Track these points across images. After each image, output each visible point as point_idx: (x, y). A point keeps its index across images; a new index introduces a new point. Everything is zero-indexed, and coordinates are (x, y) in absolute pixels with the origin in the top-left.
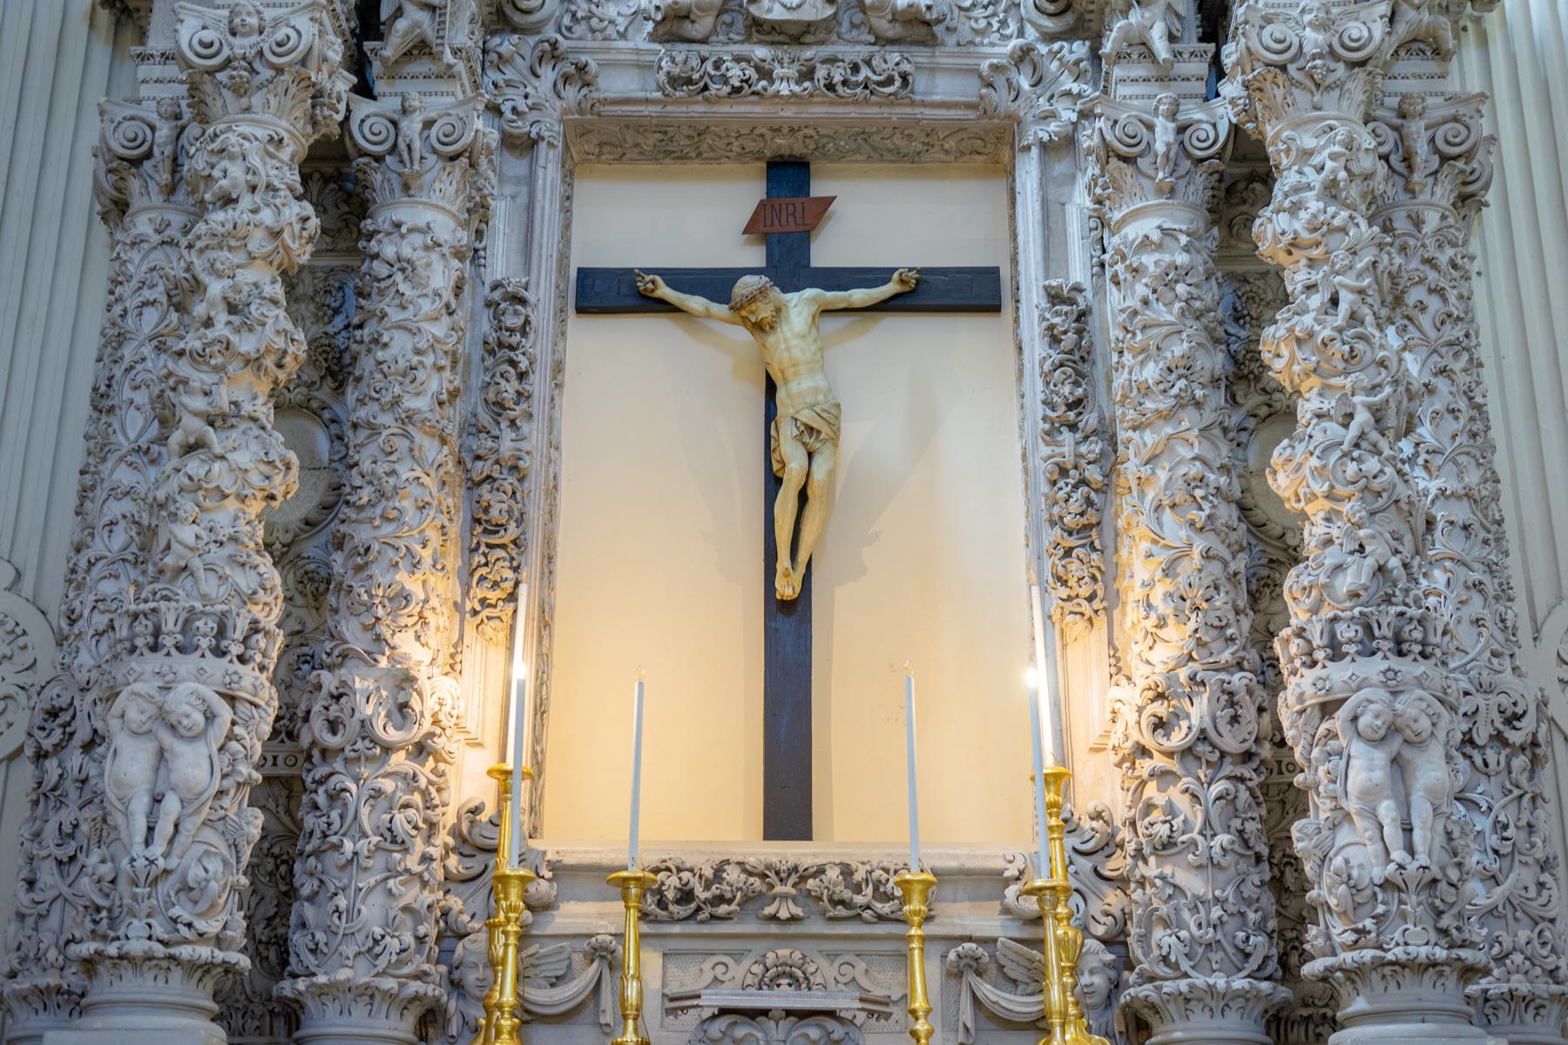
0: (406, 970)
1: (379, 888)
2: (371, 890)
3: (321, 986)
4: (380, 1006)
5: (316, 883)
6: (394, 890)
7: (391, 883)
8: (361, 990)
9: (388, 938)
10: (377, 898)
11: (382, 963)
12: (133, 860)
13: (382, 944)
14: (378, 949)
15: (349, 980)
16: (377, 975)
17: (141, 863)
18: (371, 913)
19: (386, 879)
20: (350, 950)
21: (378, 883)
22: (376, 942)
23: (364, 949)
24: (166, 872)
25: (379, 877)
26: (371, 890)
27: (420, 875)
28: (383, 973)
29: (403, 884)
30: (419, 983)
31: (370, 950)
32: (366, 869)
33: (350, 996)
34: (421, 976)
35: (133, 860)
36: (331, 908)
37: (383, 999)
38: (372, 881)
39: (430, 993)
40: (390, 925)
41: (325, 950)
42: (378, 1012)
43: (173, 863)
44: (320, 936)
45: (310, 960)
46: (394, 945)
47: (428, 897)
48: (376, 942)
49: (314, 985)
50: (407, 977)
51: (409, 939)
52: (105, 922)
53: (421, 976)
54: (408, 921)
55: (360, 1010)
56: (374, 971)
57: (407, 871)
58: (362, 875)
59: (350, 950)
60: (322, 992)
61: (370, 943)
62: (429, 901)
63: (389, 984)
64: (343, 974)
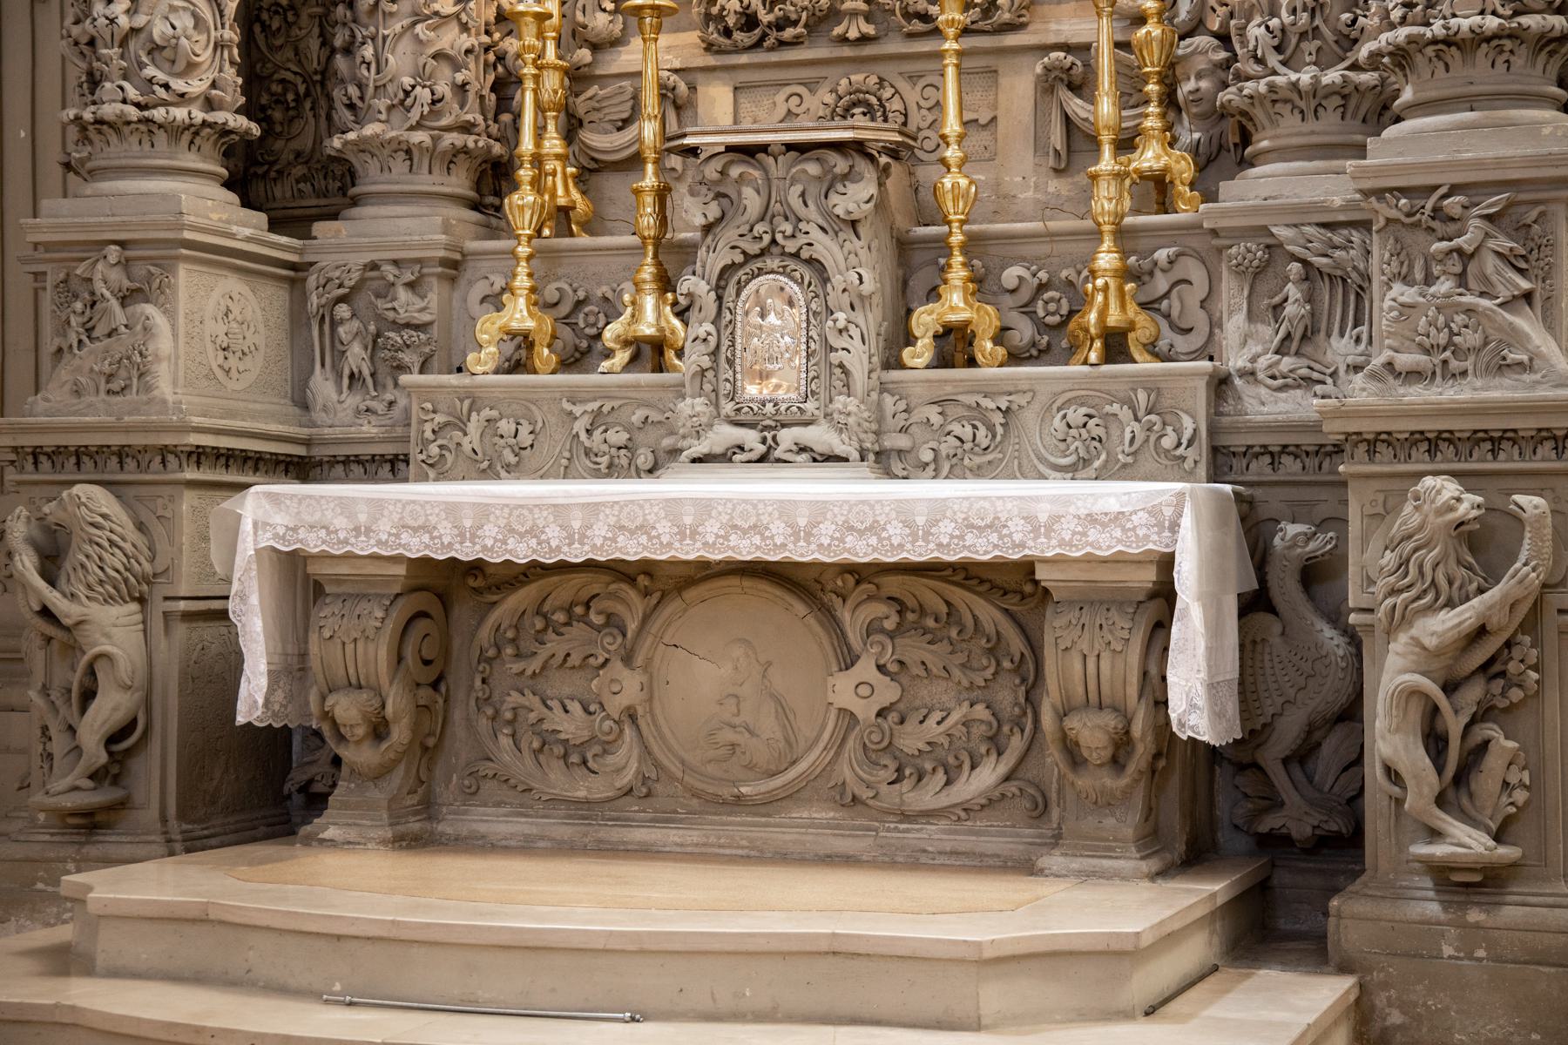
0: (444, 122)
1: (408, 34)
2: (398, 37)
3: (354, 143)
4: (421, 160)
5: (347, 33)
6: (422, 36)
7: (419, 28)
8: (394, 146)
9: (418, 89)
10: (406, 45)
11: (415, 115)
12: (95, 20)
13: (412, 94)
14: (409, 101)
15: (378, 136)
16: (412, 128)
17: (102, 21)
18: (400, 63)
19: (414, 24)
20: (381, 104)
21: (405, 30)
22: (407, 93)
23: (396, 101)
24: (134, 31)
25: (406, 22)
26: (398, 37)
27: (457, 16)
28: (418, 126)
29: (434, 28)
30: (455, 135)
31: (402, 102)
32: (391, 14)
33: (386, 152)
34: (467, 128)
35: (95, 20)
36: (359, 60)
37: (421, 153)
38: (398, 27)
39: (471, 145)
40: (422, 76)
41: (359, 104)
42: (420, 167)
43: (140, 20)
44: (353, 91)
45: (348, 115)
46: (424, 95)
47: (466, 41)
48: (407, 93)
49: (346, 143)
50: (448, 129)
51: (443, 88)
52: (85, 86)
53: (467, 128)
54: (445, 71)
55: (399, 165)
56: (408, 125)
57: (436, 13)
58: (390, 22)
59: (381, 104)
60: (362, 146)
61: (401, 95)
62: (467, 45)
63: (420, 137)
64: (370, 129)
